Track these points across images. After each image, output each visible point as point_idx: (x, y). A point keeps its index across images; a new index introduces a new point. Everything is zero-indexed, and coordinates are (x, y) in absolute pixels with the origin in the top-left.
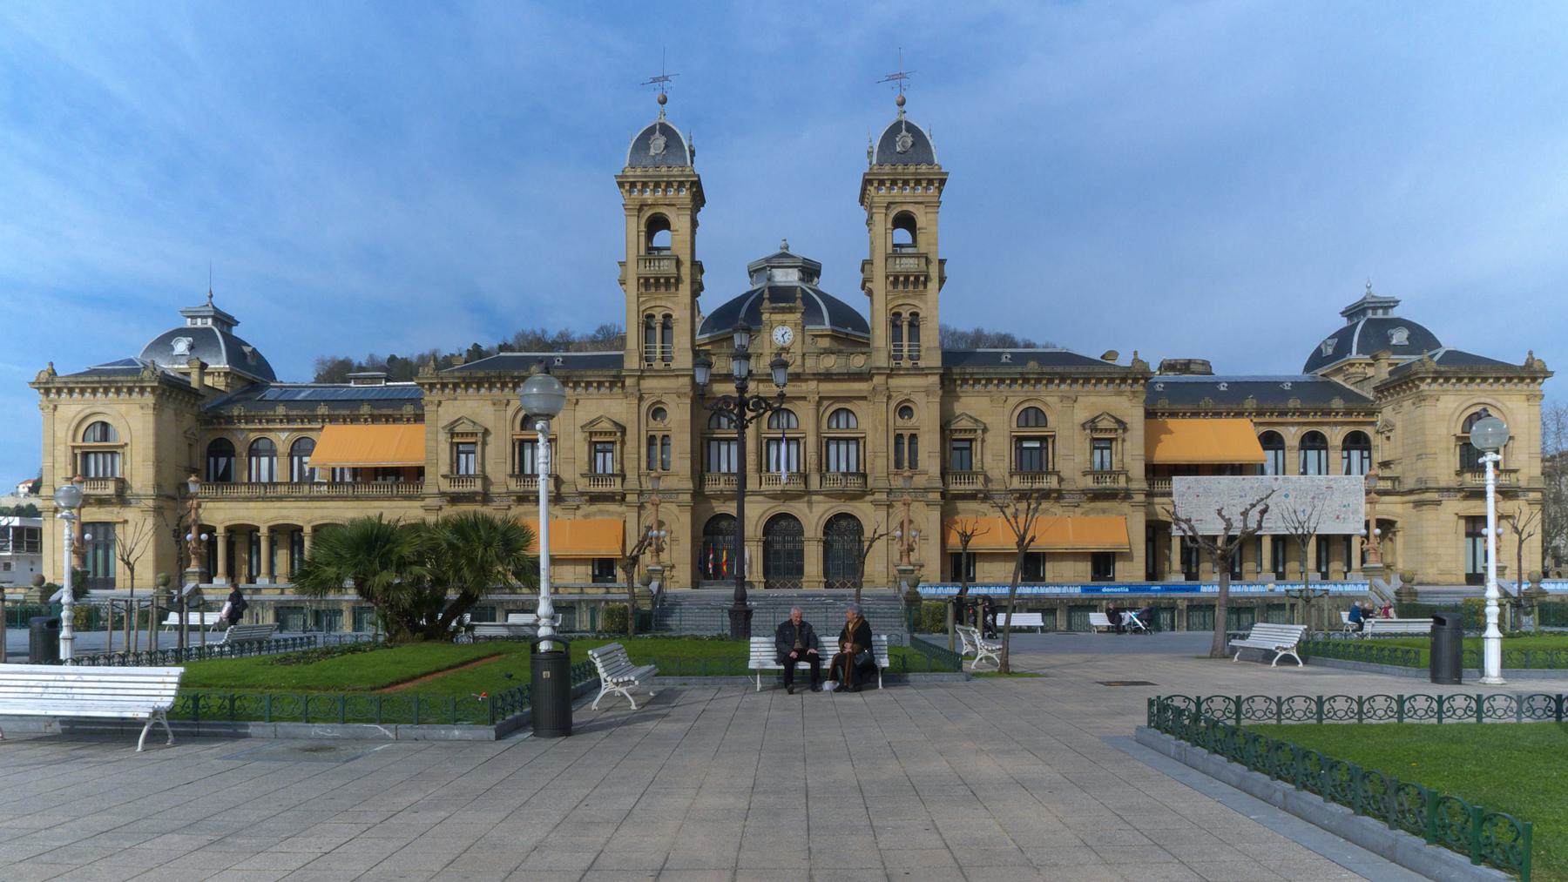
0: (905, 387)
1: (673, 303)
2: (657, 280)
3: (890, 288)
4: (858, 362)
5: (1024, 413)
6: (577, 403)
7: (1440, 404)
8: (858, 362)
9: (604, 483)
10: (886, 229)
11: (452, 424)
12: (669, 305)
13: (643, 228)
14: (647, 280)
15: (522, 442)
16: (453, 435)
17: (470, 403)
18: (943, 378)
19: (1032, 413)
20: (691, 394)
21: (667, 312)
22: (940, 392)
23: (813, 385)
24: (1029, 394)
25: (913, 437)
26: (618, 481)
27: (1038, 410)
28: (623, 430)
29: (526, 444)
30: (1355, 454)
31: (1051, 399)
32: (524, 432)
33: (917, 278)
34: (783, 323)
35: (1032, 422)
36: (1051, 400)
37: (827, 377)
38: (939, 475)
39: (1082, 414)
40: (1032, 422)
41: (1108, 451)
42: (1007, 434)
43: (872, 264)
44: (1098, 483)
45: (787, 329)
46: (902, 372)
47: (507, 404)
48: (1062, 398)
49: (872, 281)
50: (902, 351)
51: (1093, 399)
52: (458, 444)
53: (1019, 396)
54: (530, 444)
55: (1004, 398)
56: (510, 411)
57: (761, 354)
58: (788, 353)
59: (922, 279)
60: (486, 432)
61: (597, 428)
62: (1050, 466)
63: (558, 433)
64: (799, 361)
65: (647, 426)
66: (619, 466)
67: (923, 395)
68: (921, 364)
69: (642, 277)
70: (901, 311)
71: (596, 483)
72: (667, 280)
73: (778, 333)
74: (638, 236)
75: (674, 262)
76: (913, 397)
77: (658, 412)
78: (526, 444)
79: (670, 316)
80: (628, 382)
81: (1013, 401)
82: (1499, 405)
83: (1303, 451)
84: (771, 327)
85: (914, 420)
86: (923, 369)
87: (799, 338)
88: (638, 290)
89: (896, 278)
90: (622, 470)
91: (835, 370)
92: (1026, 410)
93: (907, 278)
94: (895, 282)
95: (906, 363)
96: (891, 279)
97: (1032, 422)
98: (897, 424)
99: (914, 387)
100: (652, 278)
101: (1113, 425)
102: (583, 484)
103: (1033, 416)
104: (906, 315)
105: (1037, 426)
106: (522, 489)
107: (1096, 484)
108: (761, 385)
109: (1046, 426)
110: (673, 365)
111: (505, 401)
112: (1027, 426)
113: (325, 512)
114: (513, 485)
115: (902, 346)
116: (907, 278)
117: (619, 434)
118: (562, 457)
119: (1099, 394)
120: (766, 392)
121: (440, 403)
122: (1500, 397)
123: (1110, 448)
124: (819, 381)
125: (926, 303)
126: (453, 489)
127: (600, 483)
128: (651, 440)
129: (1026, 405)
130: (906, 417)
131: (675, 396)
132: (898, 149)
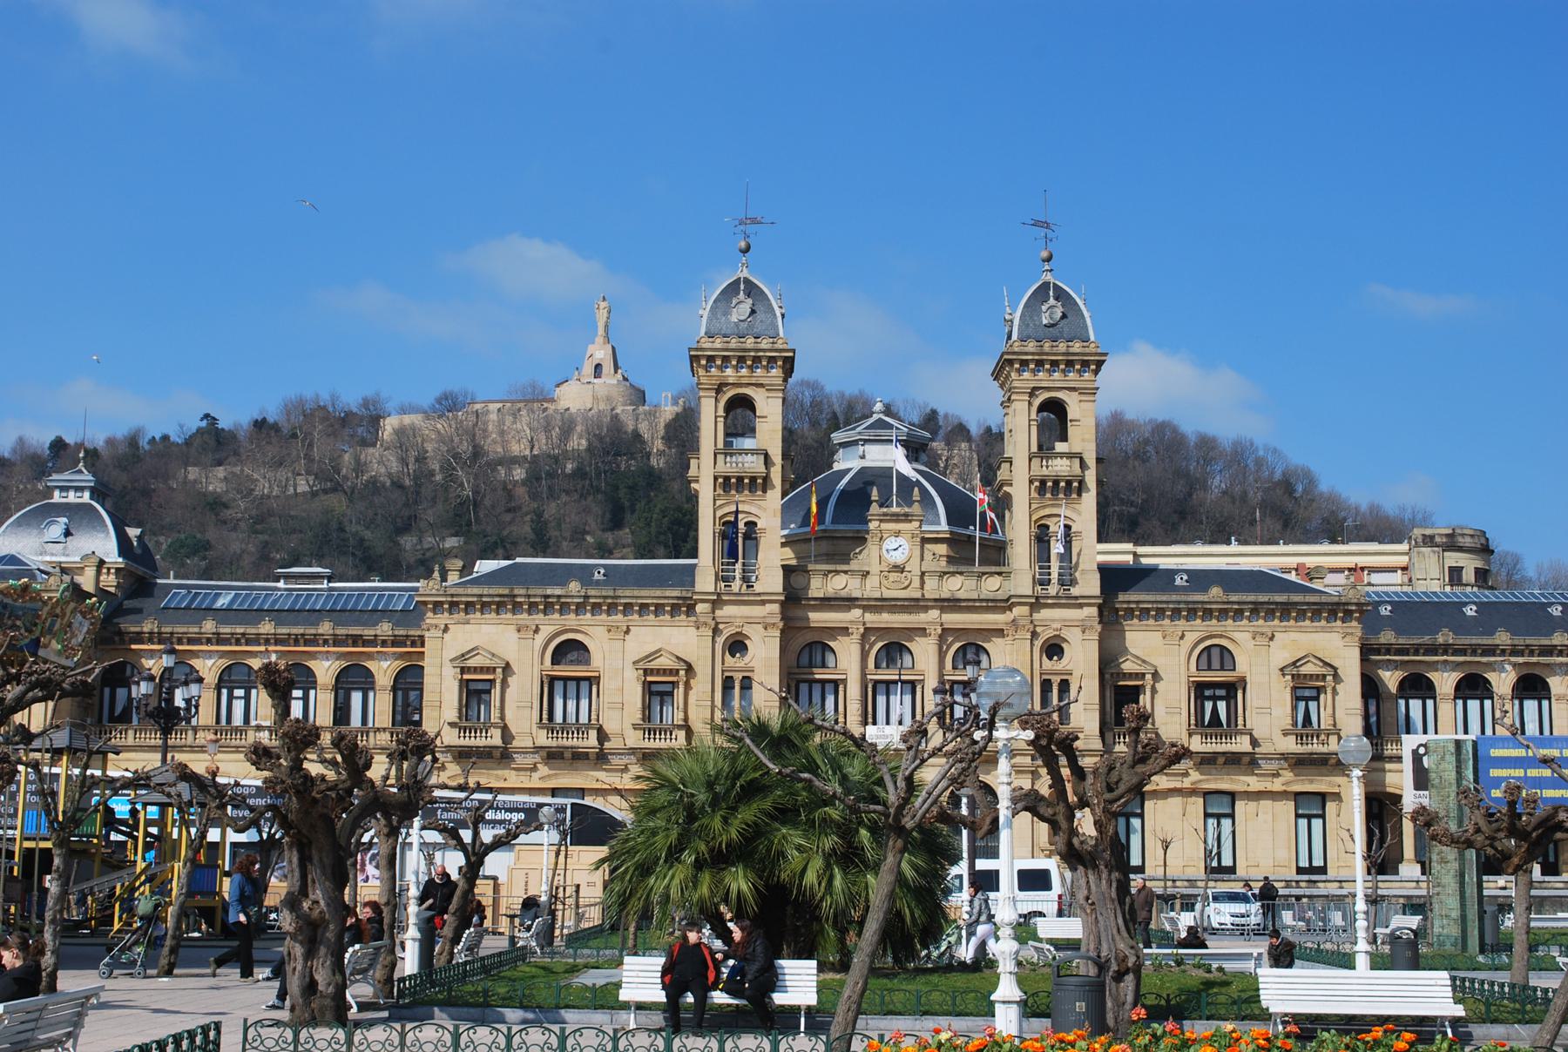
0: (1053, 620)
1: (760, 507)
2: (740, 479)
3: (1034, 495)
4: (992, 586)
5: (1205, 654)
6: (627, 632)
8: (992, 586)
9: (663, 736)
10: (1030, 421)
11: (463, 655)
12: (753, 510)
13: (721, 412)
14: (727, 479)
15: (553, 679)
16: (463, 670)
18: (1100, 608)
19: (1215, 653)
20: (781, 625)
21: (750, 519)
22: (1099, 628)
23: (934, 614)
24: (1210, 629)
25: (1064, 686)
26: (682, 734)
27: (1223, 648)
29: (556, 682)
31: (1242, 638)
32: (556, 667)
33: (1069, 483)
34: (897, 534)
35: (1216, 663)
36: (1236, 636)
37: (951, 604)
38: (1098, 733)
41: (1316, 703)
42: (1184, 680)
43: (1011, 462)
44: (1302, 744)
45: (901, 541)
46: (1050, 601)
47: (537, 631)
49: (1011, 485)
50: (1049, 574)
51: (1293, 636)
52: (468, 680)
53: (1196, 630)
54: (562, 682)
55: (1180, 634)
56: (540, 639)
57: (868, 573)
58: (902, 572)
59: (1075, 484)
61: (655, 664)
62: (1240, 721)
63: (601, 670)
64: (916, 583)
65: (723, 664)
66: (681, 715)
67: (1078, 631)
68: (1075, 591)
69: (721, 476)
70: (1048, 523)
71: (652, 736)
72: (753, 479)
73: (891, 543)
74: (716, 422)
75: (763, 457)
76: (1065, 633)
77: (737, 645)
78: (556, 682)
79: (755, 524)
80: (700, 608)
81: (1191, 638)
84: (881, 539)
85: (1065, 660)
86: (1076, 598)
87: (917, 552)
88: (715, 491)
89: (1043, 483)
90: (686, 719)
91: (962, 595)
92: (1208, 648)
93: (1056, 483)
94: (1042, 489)
95: (1053, 589)
96: (1037, 484)
97: (1216, 663)
99: (1065, 620)
100: (734, 477)
104: (1056, 528)
105: (1222, 669)
106: (554, 743)
107: (1299, 746)
108: (868, 616)
109: (1234, 670)
110: (758, 588)
111: (534, 627)
112: (1209, 669)
114: (543, 739)
115: (1049, 567)
116: (1056, 483)
117: (682, 673)
118: (606, 700)
120: (872, 622)
121: (446, 629)
124: (943, 610)
126: (462, 742)
127: (657, 736)
128: (728, 684)
130: (1055, 658)
131: (760, 627)
132: (1045, 322)
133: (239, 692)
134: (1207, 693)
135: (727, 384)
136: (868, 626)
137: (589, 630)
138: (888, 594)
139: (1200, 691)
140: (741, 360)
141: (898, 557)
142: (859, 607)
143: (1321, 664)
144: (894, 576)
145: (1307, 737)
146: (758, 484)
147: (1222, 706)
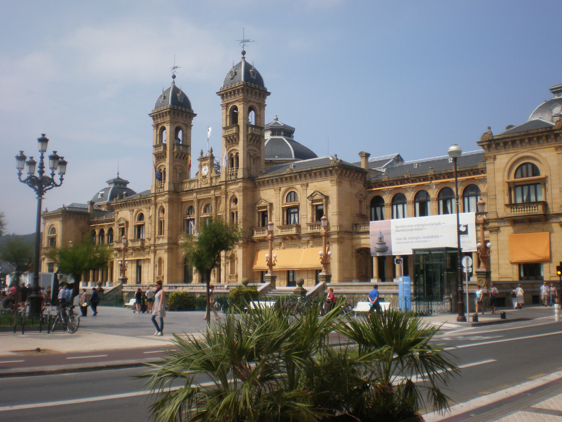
0: (232, 189)
7: (497, 162)
31: (298, 187)
34: (205, 165)
35: (293, 199)
39: (310, 192)
40: (293, 199)
44: (312, 229)
47: (133, 211)
48: (302, 185)
51: (315, 184)
56: (134, 214)
81: (283, 189)
82: (536, 156)
83: (373, 209)
92: (290, 193)
98: (160, 216)
103: (291, 195)
107: (311, 230)
112: (291, 201)
122: (537, 151)
123: (298, 212)
125: (238, 147)
129: (289, 191)
134: (292, 211)
135: (159, 124)
136: (198, 198)
137: (142, 209)
138: (203, 186)
142: (195, 192)
143: (320, 195)
144: (204, 180)
145: (318, 226)
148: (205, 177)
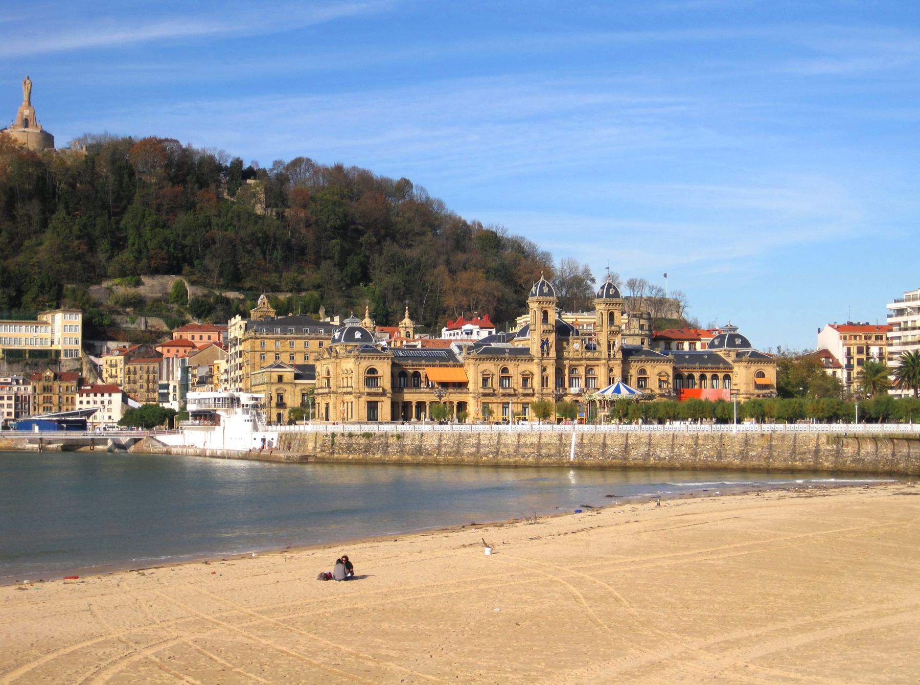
16: (483, 375)
17: (488, 365)
18: (622, 361)
23: (584, 362)
28: (533, 375)
30: (727, 381)
34: (577, 342)
37: (588, 359)
39: (656, 371)
56: (499, 367)
60: (493, 375)
73: (575, 345)
90: (532, 386)
91: (590, 357)
101: (665, 374)
102: (521, 391)
104: (612, 342)
113: (461, 398)
119: (661, 365)
133: (416, 379)
139: (639, 379)
140: (547, 302)
141: (577, 348)
146: (549, 332)
147: (643, 382)
148: (577, 351)
